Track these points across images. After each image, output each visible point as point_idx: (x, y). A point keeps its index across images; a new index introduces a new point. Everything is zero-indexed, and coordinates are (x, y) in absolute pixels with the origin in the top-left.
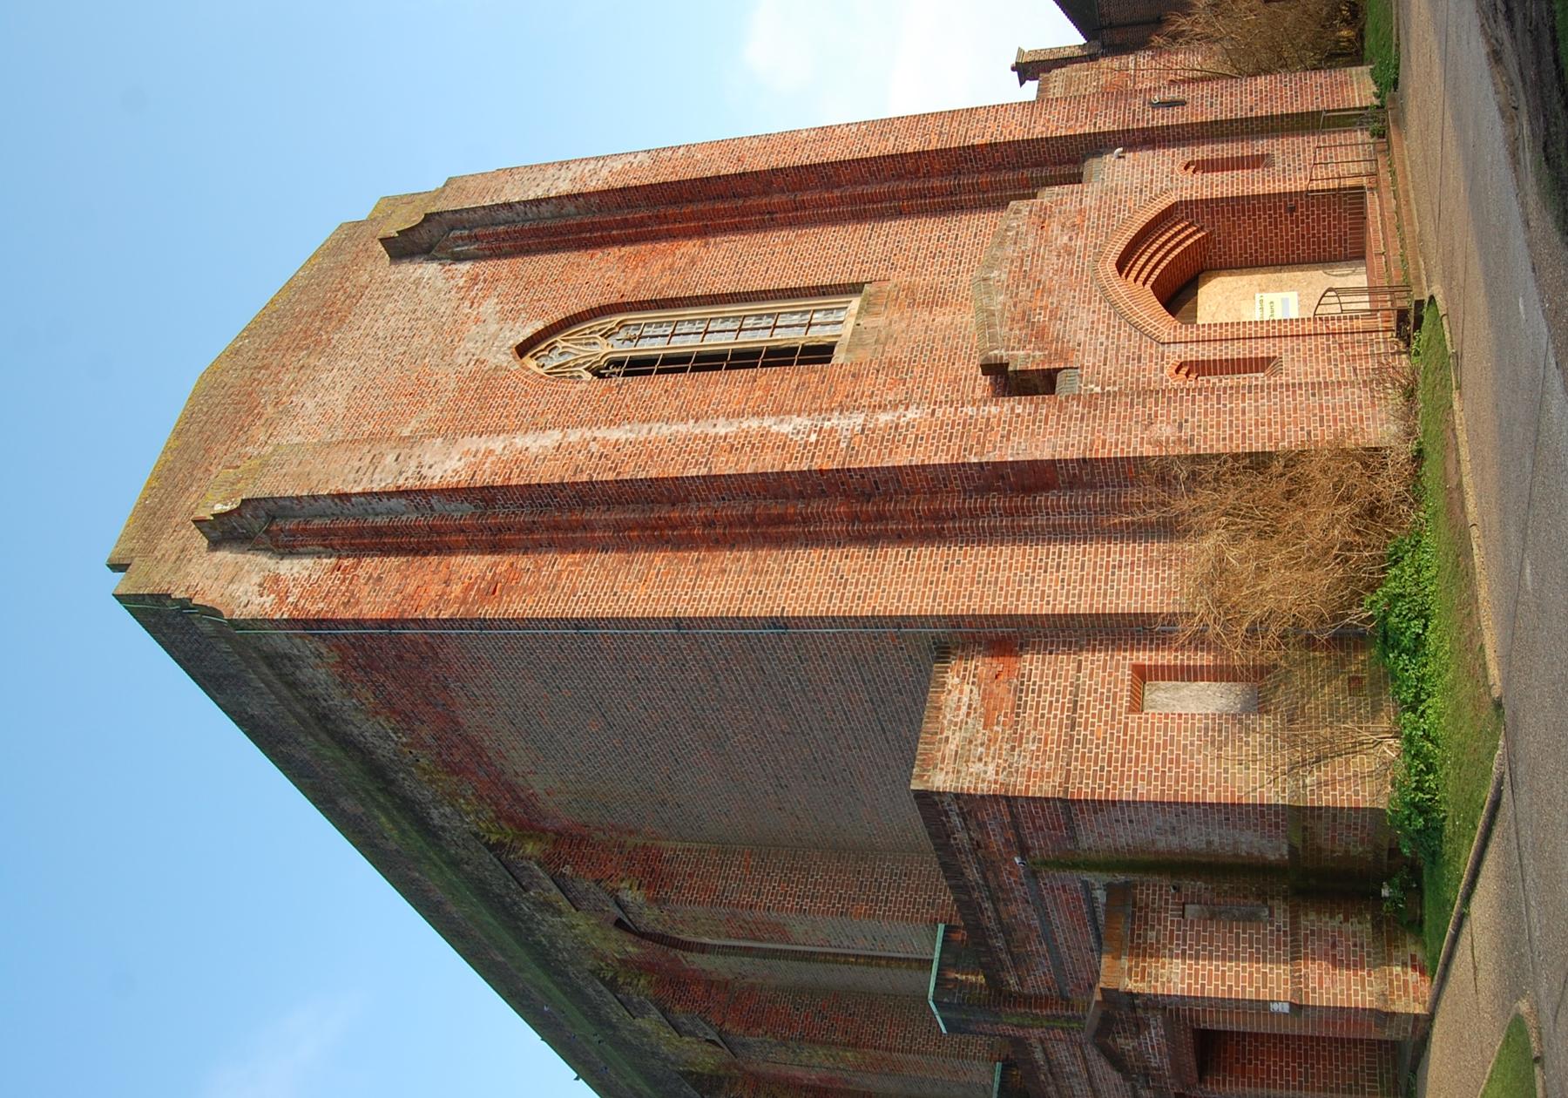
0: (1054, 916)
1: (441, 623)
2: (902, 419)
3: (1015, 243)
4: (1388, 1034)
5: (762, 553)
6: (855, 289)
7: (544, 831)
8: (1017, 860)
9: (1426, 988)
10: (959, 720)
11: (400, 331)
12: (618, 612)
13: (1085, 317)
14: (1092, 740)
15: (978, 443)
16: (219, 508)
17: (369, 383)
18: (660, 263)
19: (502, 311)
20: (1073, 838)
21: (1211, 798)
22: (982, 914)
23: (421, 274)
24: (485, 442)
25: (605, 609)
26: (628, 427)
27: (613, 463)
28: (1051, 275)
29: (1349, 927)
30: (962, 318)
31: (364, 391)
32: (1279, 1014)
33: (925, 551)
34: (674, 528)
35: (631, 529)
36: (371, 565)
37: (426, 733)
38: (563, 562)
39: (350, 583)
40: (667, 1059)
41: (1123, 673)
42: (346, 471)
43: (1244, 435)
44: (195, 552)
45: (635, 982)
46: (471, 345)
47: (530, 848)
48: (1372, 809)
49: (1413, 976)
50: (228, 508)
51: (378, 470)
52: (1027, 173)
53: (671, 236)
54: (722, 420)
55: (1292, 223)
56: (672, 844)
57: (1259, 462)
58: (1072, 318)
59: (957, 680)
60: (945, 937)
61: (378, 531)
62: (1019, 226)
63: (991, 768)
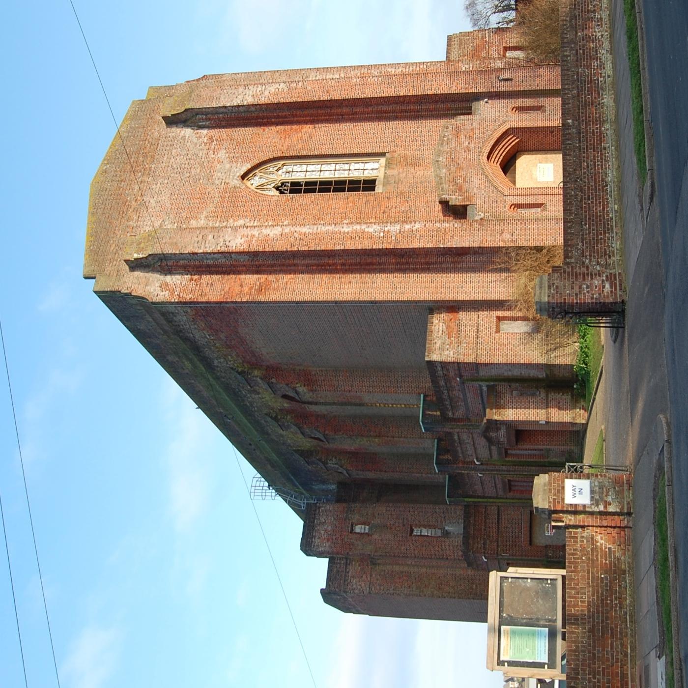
0: (468, 395)
1: (242, 302)
2: (414, 228)
3: (448, 144)
4: (575, 429)
5: (364, 275)
6: (383, 154)
7: (261, 366)
8: (458, 379)
9: (586, 415)
10: (439, 336)
11: (183, 165)
12: (313, 299)
13: (476, 182)
14: (484, 343)
15: (443, 239)
16: (136, 256)
17: (177, 192)
18: (296, 136)
19: (229, 157)
20: (478, 372)
21: (522, 362)
25: (308, 297)
26: (308, 227)
27: (306, 242)
28: (462, 161)
29: (564, 397)
30: (427, 172)
31: (176, 195)
32: (542, 424)
33: (423, 275)
34: (330, 266)
35: (313, 266)
36: (206, 279)
37: (222, 336)
38: (288, 277)
39: (200, 286)
40: (290, 445)
41: (493, 319)
42: (193, 242)
43: (534, 239)
44: (124, 272)
45: (285, 417)
46: (219, 174)
47: (256, 373)
48: (571, 365)
49: (582, 412)
50: (141, 256)
51: (207, 242)
52: (449, 105)
53: (298, 123)
54: (345, 226)
56: (315, 369)
57: (539, 249)
58: (472, 182)
59: (437, 321)
60: (424, 400)
61: (208, 266)
62: (448, 135)
63: (452, 353)
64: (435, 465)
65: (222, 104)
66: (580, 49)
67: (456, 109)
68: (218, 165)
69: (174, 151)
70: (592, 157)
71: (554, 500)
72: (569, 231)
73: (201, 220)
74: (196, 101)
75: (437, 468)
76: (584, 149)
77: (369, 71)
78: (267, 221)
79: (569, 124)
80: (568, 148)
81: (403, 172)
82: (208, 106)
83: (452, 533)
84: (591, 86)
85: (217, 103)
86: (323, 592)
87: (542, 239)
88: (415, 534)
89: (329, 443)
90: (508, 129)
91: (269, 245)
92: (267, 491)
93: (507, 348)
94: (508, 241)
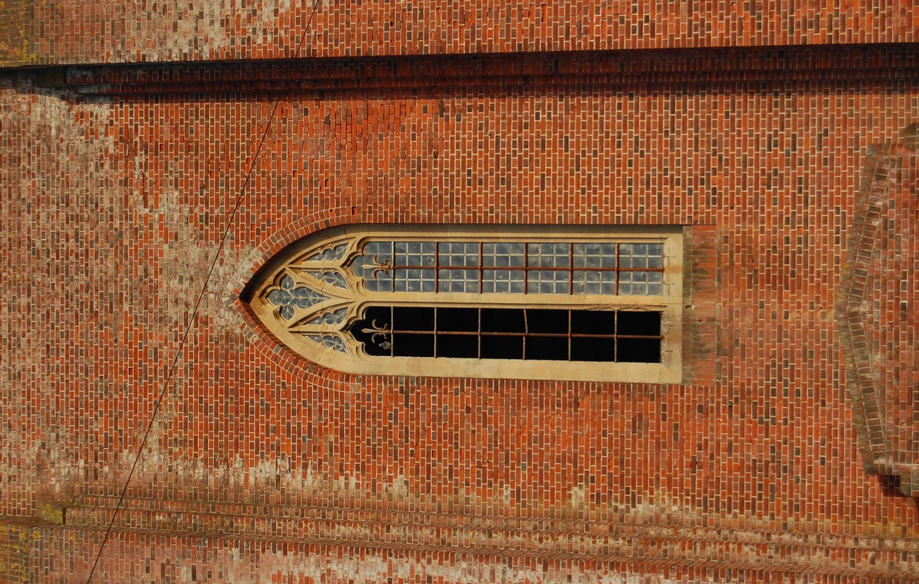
3: (885, 247)
17: (63, 344)
23: (43, 116)
24: (295, 563)
26: (464, 565)
46: (174, 283)
65: (134, 52)
68: (166, 247)
69: (25, 183)
73: (150, 451)
74: (52, 35)
78: (341, 470)
81: (744, 309)
82: (93, 61)
85: (119, 47)
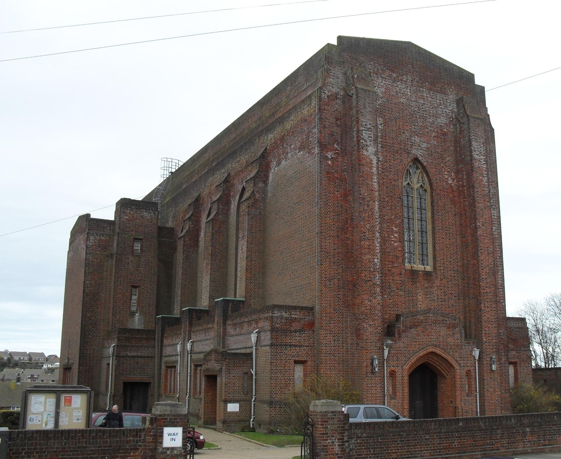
14: (286, 351)
15: (368, 318)
22: (245, 317)
41: (305, 358)
43: (368, 390)
55: (448, 402)
64: (188, 308)
66: (516, 430)
67: (470, 327)
70: (433, 443)
71: (166, 419)
72: (376, 426)
75: (185, 310)
76: (440, 436)
77: (498, 258)
78: (382, 178)
79: (459, 424)
80: (441, 423)
83: (133, 319)
84: (488, 440)
86: (88, 215)
87: (369, 397)
88: (133, 290)
89: (206, 223)
90: (454, 368)
91: (364, 180)
92: (168, 171)
93: (282, 370)
94: (366, 370)
